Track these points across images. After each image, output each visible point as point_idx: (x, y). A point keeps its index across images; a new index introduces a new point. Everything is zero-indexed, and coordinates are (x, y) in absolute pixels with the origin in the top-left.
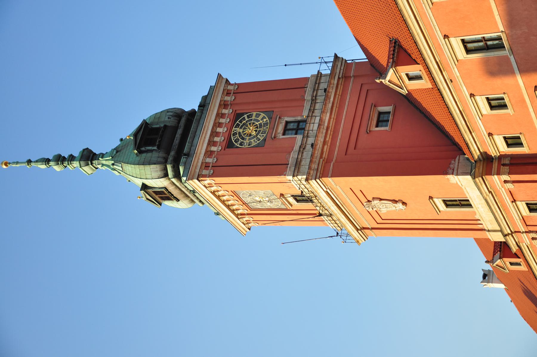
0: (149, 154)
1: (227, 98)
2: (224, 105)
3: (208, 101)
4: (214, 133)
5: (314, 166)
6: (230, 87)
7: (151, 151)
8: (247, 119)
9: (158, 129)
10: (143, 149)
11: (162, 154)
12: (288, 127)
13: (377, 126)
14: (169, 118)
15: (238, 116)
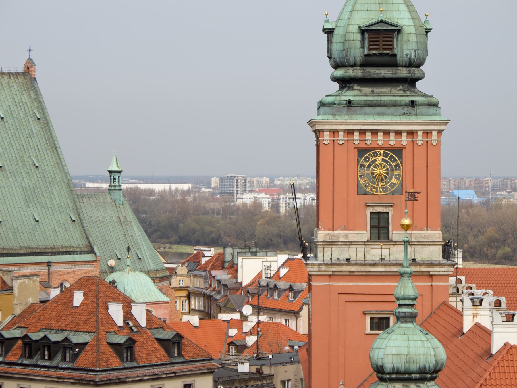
0: (358, 44)
1: (420, 138)
2: (411, 133)
3: (420, 110)
4: (374, 133)
5: (323, 268)
6: (435, 134)
7: (363, 47)
8: (393, 164)
9: (391, 47)
10: (366, 35)
11: (359, 59)
12: (382, 216)
13: (372, 319)
14: (407, 55)
15: (398, 152)
